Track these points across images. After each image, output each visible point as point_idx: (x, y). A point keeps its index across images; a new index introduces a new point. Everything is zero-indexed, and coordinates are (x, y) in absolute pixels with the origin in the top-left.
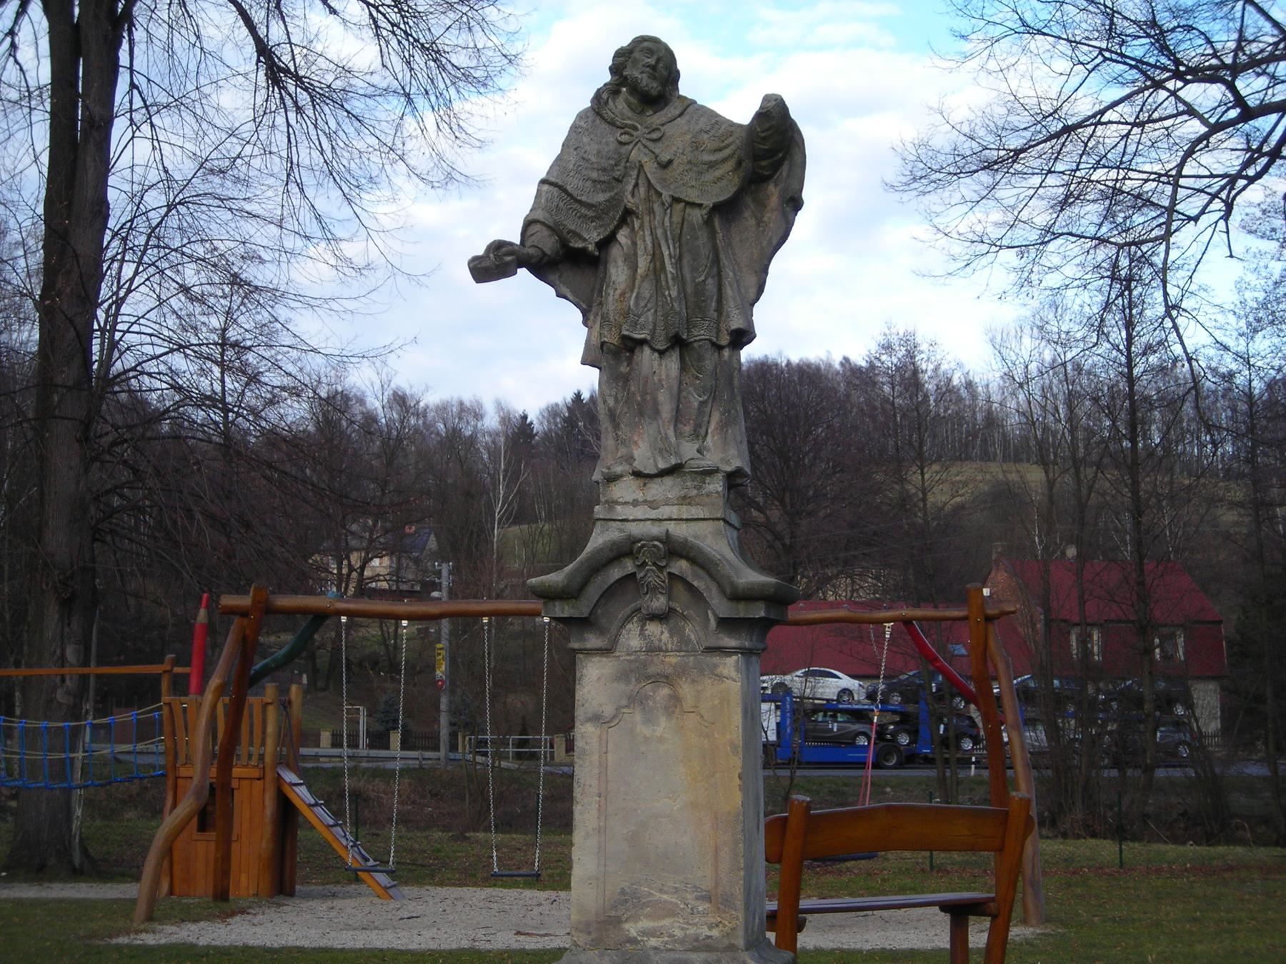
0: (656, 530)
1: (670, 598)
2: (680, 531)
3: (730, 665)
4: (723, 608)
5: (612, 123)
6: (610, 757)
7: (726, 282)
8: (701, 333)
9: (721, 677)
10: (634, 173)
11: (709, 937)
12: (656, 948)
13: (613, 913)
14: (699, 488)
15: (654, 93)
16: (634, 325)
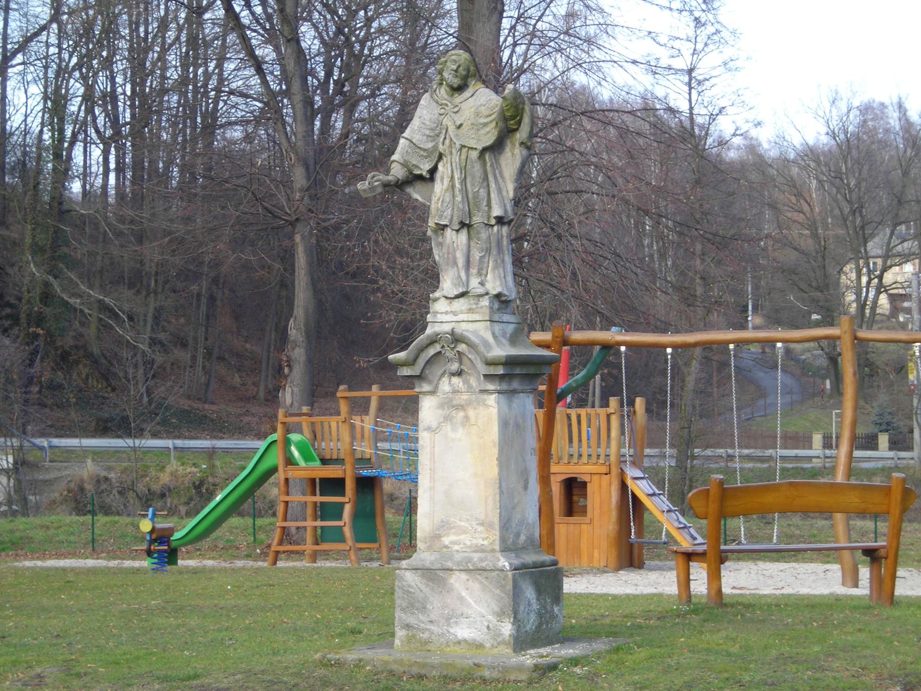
3: (492, 399)
4: (483, 369)
7: (491, 190)
8: (477, 219)
9: (488, 406)
10: (444, 131)
11: (483, 545)
12: (457, 551)
13: (438, 533)
14: (477, 304)
15: (455, 86)
16: (441, 217)
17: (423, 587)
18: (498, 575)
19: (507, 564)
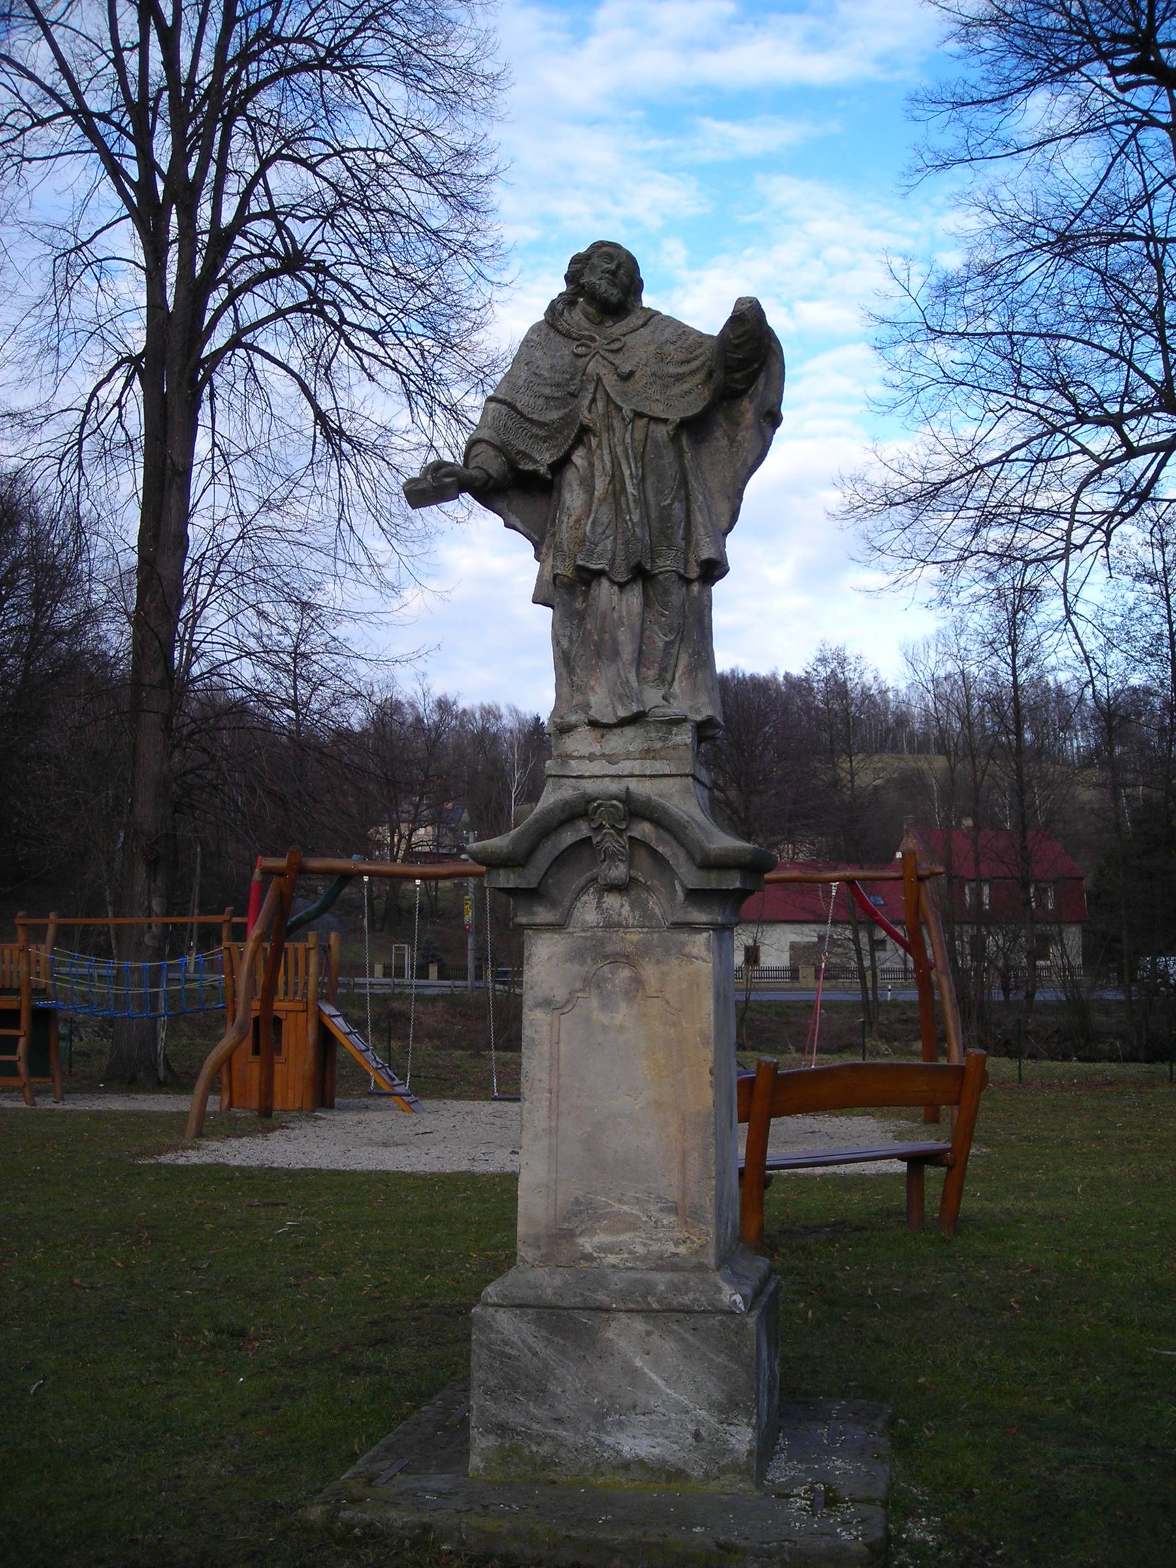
0: (614, 787)
1: (631, 866)
2: (641, 788)
4: (691, 877)
5: (567, 335)
6: (562, 1047)
8: (666, 564)
10: (591, 387)
11: (676, 1255)
12: (614, 1266)
17: (539, 1346)
18: (722, 1323)
19: (738, 1298)
